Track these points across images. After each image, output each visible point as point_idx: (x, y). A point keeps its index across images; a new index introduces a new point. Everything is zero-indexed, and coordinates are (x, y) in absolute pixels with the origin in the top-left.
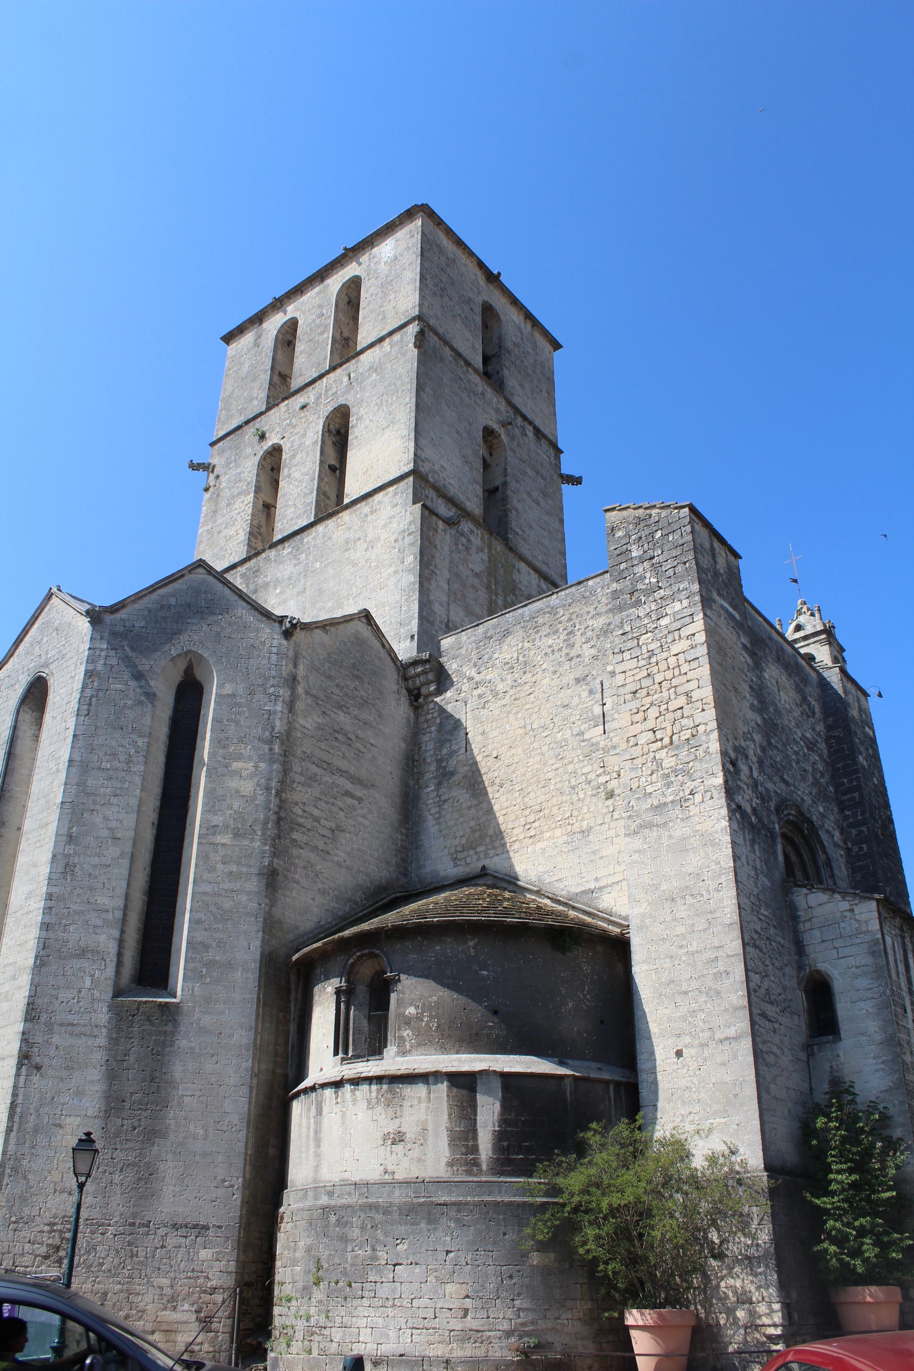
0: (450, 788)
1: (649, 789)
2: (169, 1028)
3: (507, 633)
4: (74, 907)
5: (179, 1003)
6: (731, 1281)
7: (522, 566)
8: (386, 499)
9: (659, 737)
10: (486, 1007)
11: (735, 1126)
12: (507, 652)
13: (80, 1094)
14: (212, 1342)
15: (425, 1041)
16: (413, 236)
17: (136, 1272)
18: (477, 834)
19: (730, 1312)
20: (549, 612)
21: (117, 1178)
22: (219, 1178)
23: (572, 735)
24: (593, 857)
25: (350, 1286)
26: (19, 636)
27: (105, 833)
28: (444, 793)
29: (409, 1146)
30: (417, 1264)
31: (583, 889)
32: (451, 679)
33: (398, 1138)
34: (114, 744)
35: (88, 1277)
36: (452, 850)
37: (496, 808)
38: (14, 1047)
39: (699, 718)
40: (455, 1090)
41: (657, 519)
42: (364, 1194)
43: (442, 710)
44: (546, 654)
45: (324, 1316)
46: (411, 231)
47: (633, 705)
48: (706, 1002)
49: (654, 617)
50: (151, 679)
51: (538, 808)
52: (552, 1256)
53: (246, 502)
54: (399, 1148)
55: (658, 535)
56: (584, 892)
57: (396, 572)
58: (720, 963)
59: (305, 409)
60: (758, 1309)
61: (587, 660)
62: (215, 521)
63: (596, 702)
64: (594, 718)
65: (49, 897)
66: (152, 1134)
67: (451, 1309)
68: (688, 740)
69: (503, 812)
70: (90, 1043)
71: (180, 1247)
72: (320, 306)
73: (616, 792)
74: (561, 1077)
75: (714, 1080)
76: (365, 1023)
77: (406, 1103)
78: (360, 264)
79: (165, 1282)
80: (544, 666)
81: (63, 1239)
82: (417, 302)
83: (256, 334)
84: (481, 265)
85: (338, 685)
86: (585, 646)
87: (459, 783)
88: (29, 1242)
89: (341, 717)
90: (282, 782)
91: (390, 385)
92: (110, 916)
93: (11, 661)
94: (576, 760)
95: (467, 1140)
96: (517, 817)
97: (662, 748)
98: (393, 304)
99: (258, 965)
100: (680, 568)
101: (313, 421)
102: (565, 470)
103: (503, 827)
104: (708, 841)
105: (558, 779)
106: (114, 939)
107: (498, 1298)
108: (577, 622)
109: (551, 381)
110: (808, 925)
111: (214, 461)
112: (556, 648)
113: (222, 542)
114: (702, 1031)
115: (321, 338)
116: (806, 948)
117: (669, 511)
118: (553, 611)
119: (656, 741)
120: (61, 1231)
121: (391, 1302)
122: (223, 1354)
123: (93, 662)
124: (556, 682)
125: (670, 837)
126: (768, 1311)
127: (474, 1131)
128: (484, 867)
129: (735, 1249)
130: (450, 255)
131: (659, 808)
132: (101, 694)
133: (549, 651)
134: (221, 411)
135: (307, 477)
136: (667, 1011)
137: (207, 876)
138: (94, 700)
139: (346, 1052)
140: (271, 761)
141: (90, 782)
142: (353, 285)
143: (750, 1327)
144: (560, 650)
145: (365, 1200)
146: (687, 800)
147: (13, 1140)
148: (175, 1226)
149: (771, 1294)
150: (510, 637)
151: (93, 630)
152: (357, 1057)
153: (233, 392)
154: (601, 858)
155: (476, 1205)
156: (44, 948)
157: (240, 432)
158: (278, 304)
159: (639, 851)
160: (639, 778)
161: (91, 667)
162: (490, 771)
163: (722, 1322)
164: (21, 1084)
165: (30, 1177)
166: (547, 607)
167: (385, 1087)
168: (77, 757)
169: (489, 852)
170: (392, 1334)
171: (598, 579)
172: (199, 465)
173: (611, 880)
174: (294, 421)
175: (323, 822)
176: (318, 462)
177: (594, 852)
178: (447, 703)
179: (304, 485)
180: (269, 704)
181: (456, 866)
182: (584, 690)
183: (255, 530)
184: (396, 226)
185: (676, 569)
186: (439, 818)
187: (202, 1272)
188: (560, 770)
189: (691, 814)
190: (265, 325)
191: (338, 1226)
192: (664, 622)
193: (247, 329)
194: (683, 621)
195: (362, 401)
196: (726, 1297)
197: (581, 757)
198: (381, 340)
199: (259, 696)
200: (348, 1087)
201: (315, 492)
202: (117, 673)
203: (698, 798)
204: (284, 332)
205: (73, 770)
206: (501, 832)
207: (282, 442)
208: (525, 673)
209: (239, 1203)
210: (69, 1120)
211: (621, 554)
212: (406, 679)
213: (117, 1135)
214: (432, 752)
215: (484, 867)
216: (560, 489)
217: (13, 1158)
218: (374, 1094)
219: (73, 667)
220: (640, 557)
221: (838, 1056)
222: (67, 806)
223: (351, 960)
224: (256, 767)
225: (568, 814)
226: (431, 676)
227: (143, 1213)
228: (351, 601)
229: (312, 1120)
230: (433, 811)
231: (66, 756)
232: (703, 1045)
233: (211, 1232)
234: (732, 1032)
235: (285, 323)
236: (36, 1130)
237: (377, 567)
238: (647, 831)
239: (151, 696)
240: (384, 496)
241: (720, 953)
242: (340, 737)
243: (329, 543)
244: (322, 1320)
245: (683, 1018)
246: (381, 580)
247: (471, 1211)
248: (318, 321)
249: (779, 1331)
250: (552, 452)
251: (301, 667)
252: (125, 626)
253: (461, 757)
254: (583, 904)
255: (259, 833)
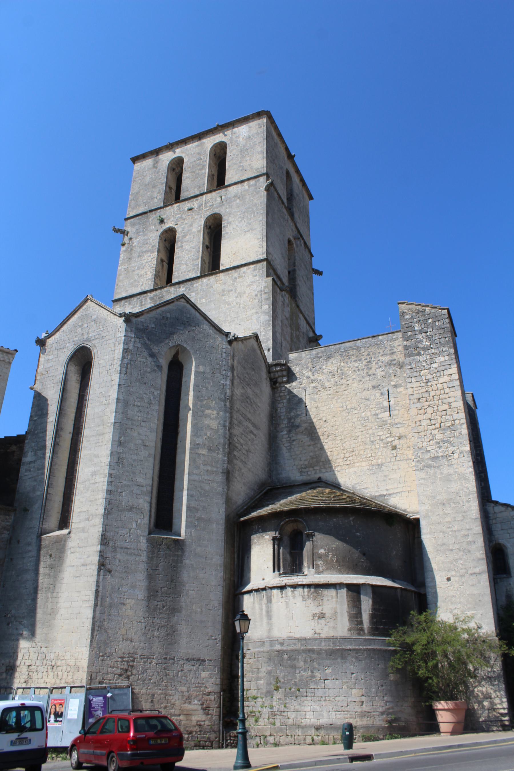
0: (297, 434)
1: (429, 448)
2: (180, 553)
3: (330, 357)
4: (124, 483)
5: (184, 540)
6: (480, 688)
7: (301, 316)
8: (249, 271)
9: (433, 423)
10: (360, 551)
11: (480, 615)
12: (332, 365)
13: (133, 587)
14: (210, 720)
15: (330, 567)
16: (261, 127)
17: (169, 684)
18: (315, 460)
19: (480, 703)
20: (356, 349)
21: (156, 633)
22: (209, 635)
23: (371, 415)
24: (385, 478)
25: (299, 690)
26: (64, 320)
27: (139, 442)
28: (293, 436)
29: (327, 620)
30: (337, 679)
31: (379, 494)
32: (295, 376)
33: (322, 616)
34: (141, 392)
35: (144, 686)
36: (299, 467)
37: (326, 447)
38: (96, 559)
39: (456, 416)
40: (350, 593)
41: (429, 313)
42: (304, 644)
43: (290, 392)
44: (354, 371)
45: (283, 706)
46: (259, 124)
47: (419, 405)
48: (463, 555)
49: (429, 362)
50: (160, 358)
51: (351, 450)
52: (398, 675)
53: (152, 257)
54: (322, 621)
55: (430, 321)
56: (380, 495)
57: (257, 313)
58: (470, 537)
59: (191, 211)
60: (495, 701)
61: (379, 377)
62: (130, 264)
63: (385, 400)
64: (384, 408)
65: (110, 475)
66: (174, 610)
67: (355, 702)
68: (450, 426)
69: (331, 450)
70: (137, 559)
71: (191, 671)
72: (199, 154)
73: (398, 447)
74: (396, 588)
75: (468, 593)
76: (288, 556)
77: (325, 599)
78: (225, 135)
79: (184, 689)
80: (354, 377)
81: (129, 666)
82: (265, 165)
83: (154, 160)
84: (287, 149)
85: (247, 373)
86: (378, 370)
87: (303, 432)
88: (111, 667)
89: (249, 391)
90: (230, 423)
91: (249, 208)
92: (144, 489)
93: (57, 334)
94: (374, 428)
95: (357, 618)
96: (339, 453)
97: (435, 429)
98: (248, 163)
99: (224, 522)
100: (443, 340)
101: (197, 219)
102: (315, 266)
103: (330, 458)
104: (462, 477)
105: (363, 437)
106: (147, 502)
107: (377, 696)
108: (373, 356)
109: (308, 216)
110: (494, 521)
111: (128, 229)
112: (360, 369)
113: (136, 277)
114: (461, 569)
115: (201, 172)
116: (493, 532)
117: (436, 310)
118: (358, 349)
119: (432, 425)
120: (128, 662)
121: (324, 699)
122: (216, 726)
123: (127, 344)
124: (361, 386)
125: (441, 473)
126: (500, 702)
127: (360, 613)
128: (320, 478)
129: (482, 673)
130: (276, 141)
131: (435, 458)
132: (132, 363)
133: (356, 369)
134: (131, 200)
135: (194, 250)
136: (442, 558)
137: (195, 471)
138: (129, 365)
139: (279, 571)
140: (225, 411)
141: (129, 412)
142: (219, 146)
143: (491, 710)
144: (363, 370)
145: (305, 647)
146: (450, 456)
147: (98, 611)
148: (188, 660)
149: (502, 694)
150: (333, 359)
151: (126, 326)
152: (285, 573)
153: (139, 192)
154: (390, 479)
155: (365, 650)
156: (109, 504)
157: (146, 215)
158: (170, 147)
159: (424, 479)
160: (423, 442)
161: (126, 347)
162: (321, 428)
163: (476, 707)
164: (101, 580)
165: (109, 631)
166: (355, 346)
167: (312, 590)
168: (121, 397)
169: (322, 470)
170: (325, 714)
171: (385, 336)
172: (119, 230)
173: (395, 491)
174: (184, 216)
175: (244, 446)
176: (201, 243)
177: (385, 476)
178: (293, 389)
179: (192, 254)
180: (223, 380)
181: (301, 475)
182: (377, 393)
183: (157, 273)
184: (250, 119)
185: (441, 340)
186: (290, 449)
187: (203, 684)
188: (364, 432)
189: (453, 463)
190: (160, 157)
191: (290, 660)
192: (434, 366)
193: (148, 156)
194: (445, 367)
195: (230, 213)
196: (478, 695)
197: (377, 427)
198: (242, 182)
199: (217, 375)
200: (289, 589)
201: (200, 259)
202: (141, 352)
203: (456, 456)
204: (172, 163)
205: (120, 404)
206: (329, 460)
207: (176, 227)
208: (342, 379)
209: (220, 648)
210: (128, 601)
211: (408, 327)
212: (269, 372)
213: (155, 610)
214: (284, 414)
215: (320, 478)
216: (312, 276)
217: (99, 621)
218: (306, 593)
219: (112, 345)
220: (420, 331)
221: (510, 584)
222: (117, 424)
223: (283, 523)
224: (218, 414)
225: (370, 455)
226: (285, 373)
227: (171, 653)
228: (227, 324)
229: (264, 606)
230: (286, 445)
231: (115, 396)
232: (462, 576)
233: (206, 663)
234: (477, 570)
235: (174, 159)
236: (111, 606)
237: (244, 308)
238: (428, 469)
239: (160, 367)
240: (247, 270)
241: (470, 532)
242: (249, 401)
243: (211, 289)
244: (282, 708)
245: (451, 562)
246: (247, 315)
247: (363, 653)
248: (197, 162)
249: (506, 711)
250: (309, 256)
251: (235, 361)
252: (143, 326)
253: (303, 418)
254: (380, 501)
255: (221, 450)
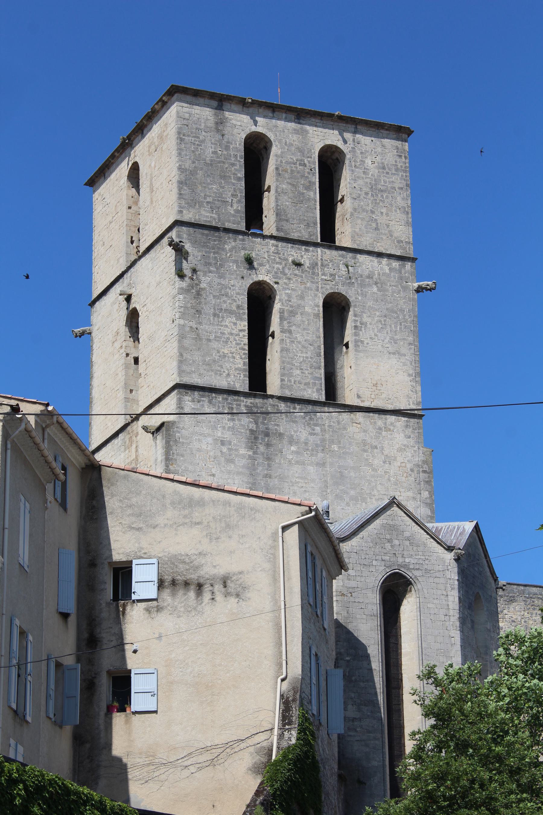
135: (312, 348)
174: (287, 271)
198: (380, 255)
207: (275, 286)
